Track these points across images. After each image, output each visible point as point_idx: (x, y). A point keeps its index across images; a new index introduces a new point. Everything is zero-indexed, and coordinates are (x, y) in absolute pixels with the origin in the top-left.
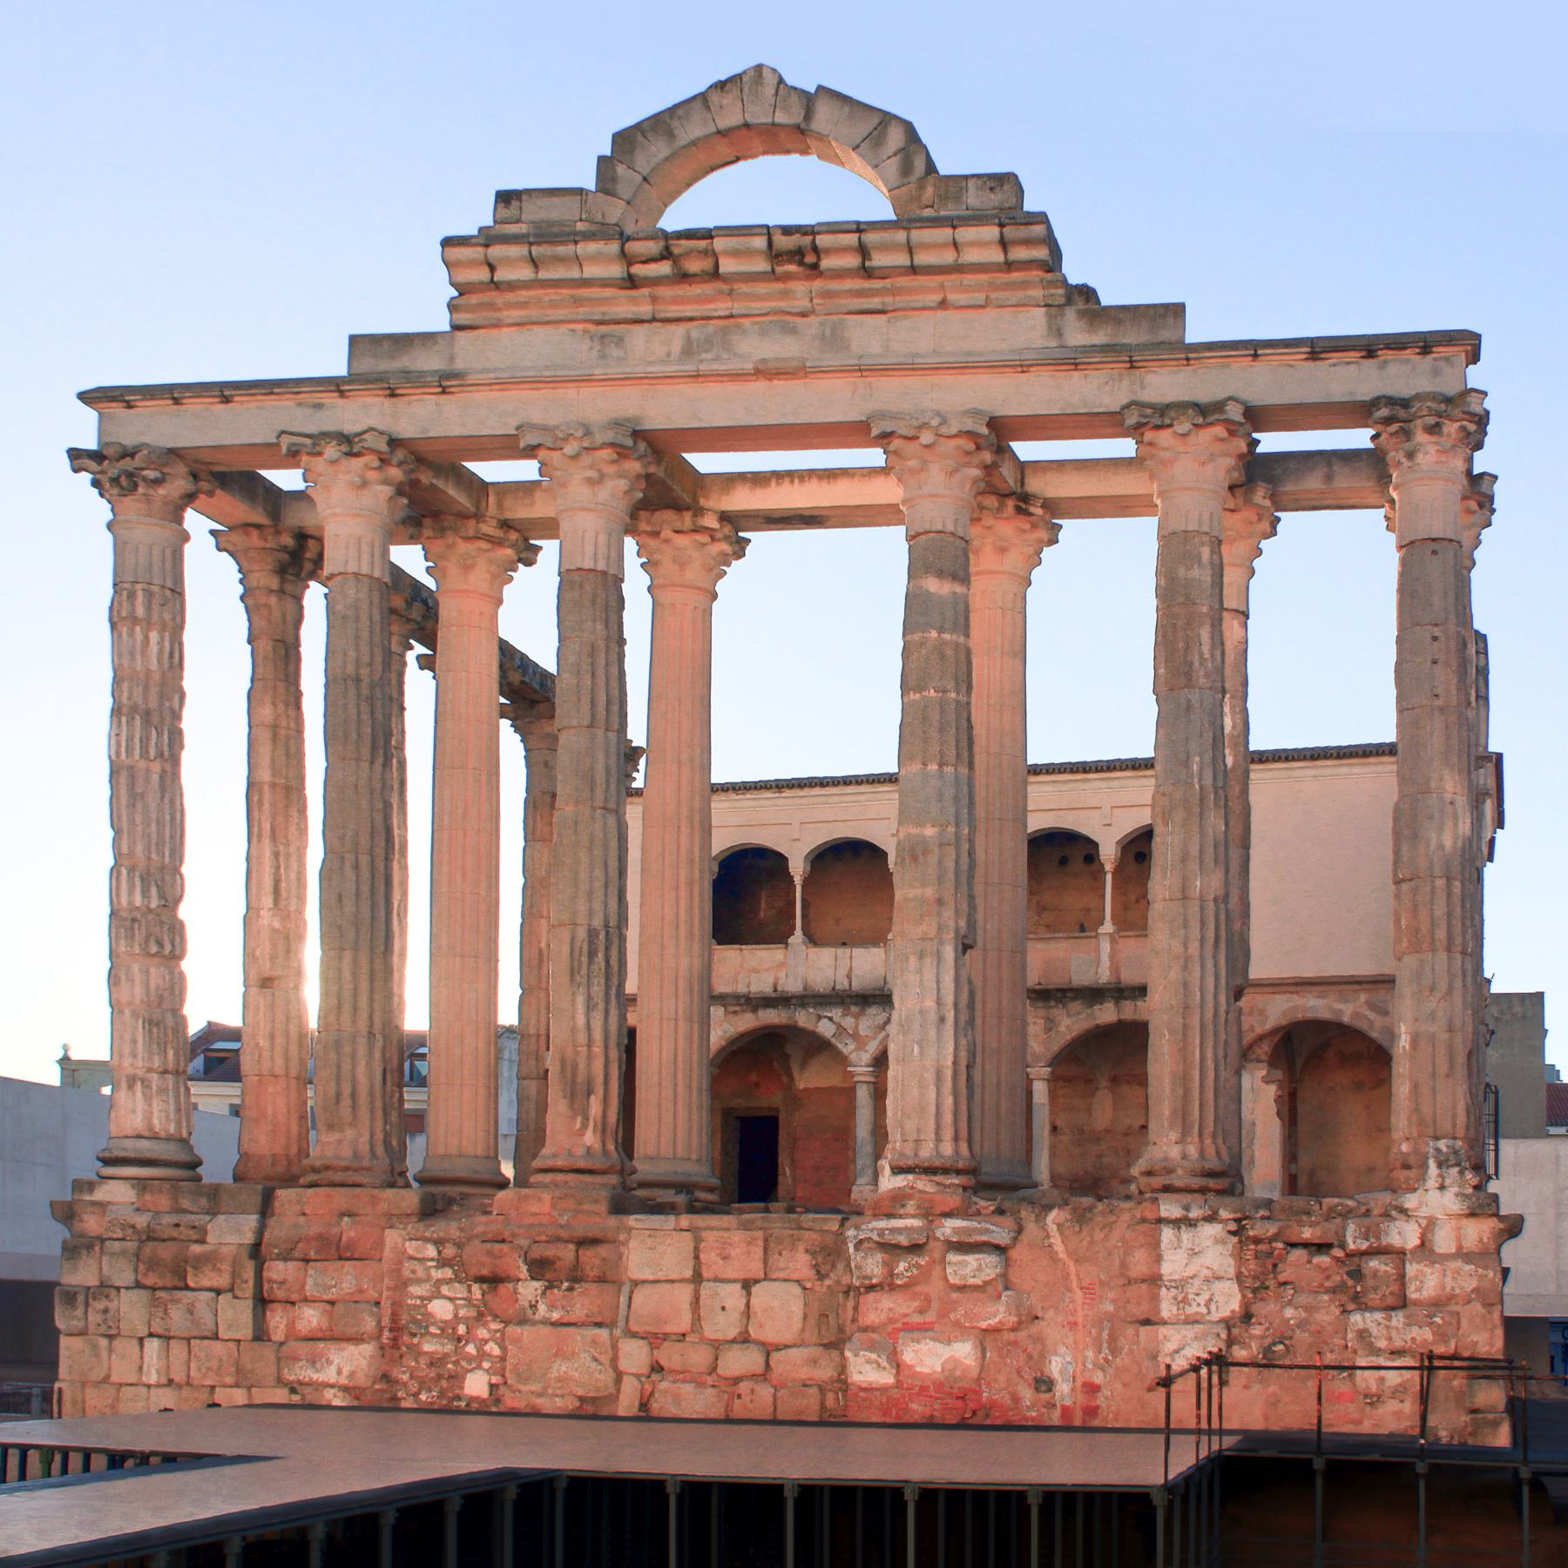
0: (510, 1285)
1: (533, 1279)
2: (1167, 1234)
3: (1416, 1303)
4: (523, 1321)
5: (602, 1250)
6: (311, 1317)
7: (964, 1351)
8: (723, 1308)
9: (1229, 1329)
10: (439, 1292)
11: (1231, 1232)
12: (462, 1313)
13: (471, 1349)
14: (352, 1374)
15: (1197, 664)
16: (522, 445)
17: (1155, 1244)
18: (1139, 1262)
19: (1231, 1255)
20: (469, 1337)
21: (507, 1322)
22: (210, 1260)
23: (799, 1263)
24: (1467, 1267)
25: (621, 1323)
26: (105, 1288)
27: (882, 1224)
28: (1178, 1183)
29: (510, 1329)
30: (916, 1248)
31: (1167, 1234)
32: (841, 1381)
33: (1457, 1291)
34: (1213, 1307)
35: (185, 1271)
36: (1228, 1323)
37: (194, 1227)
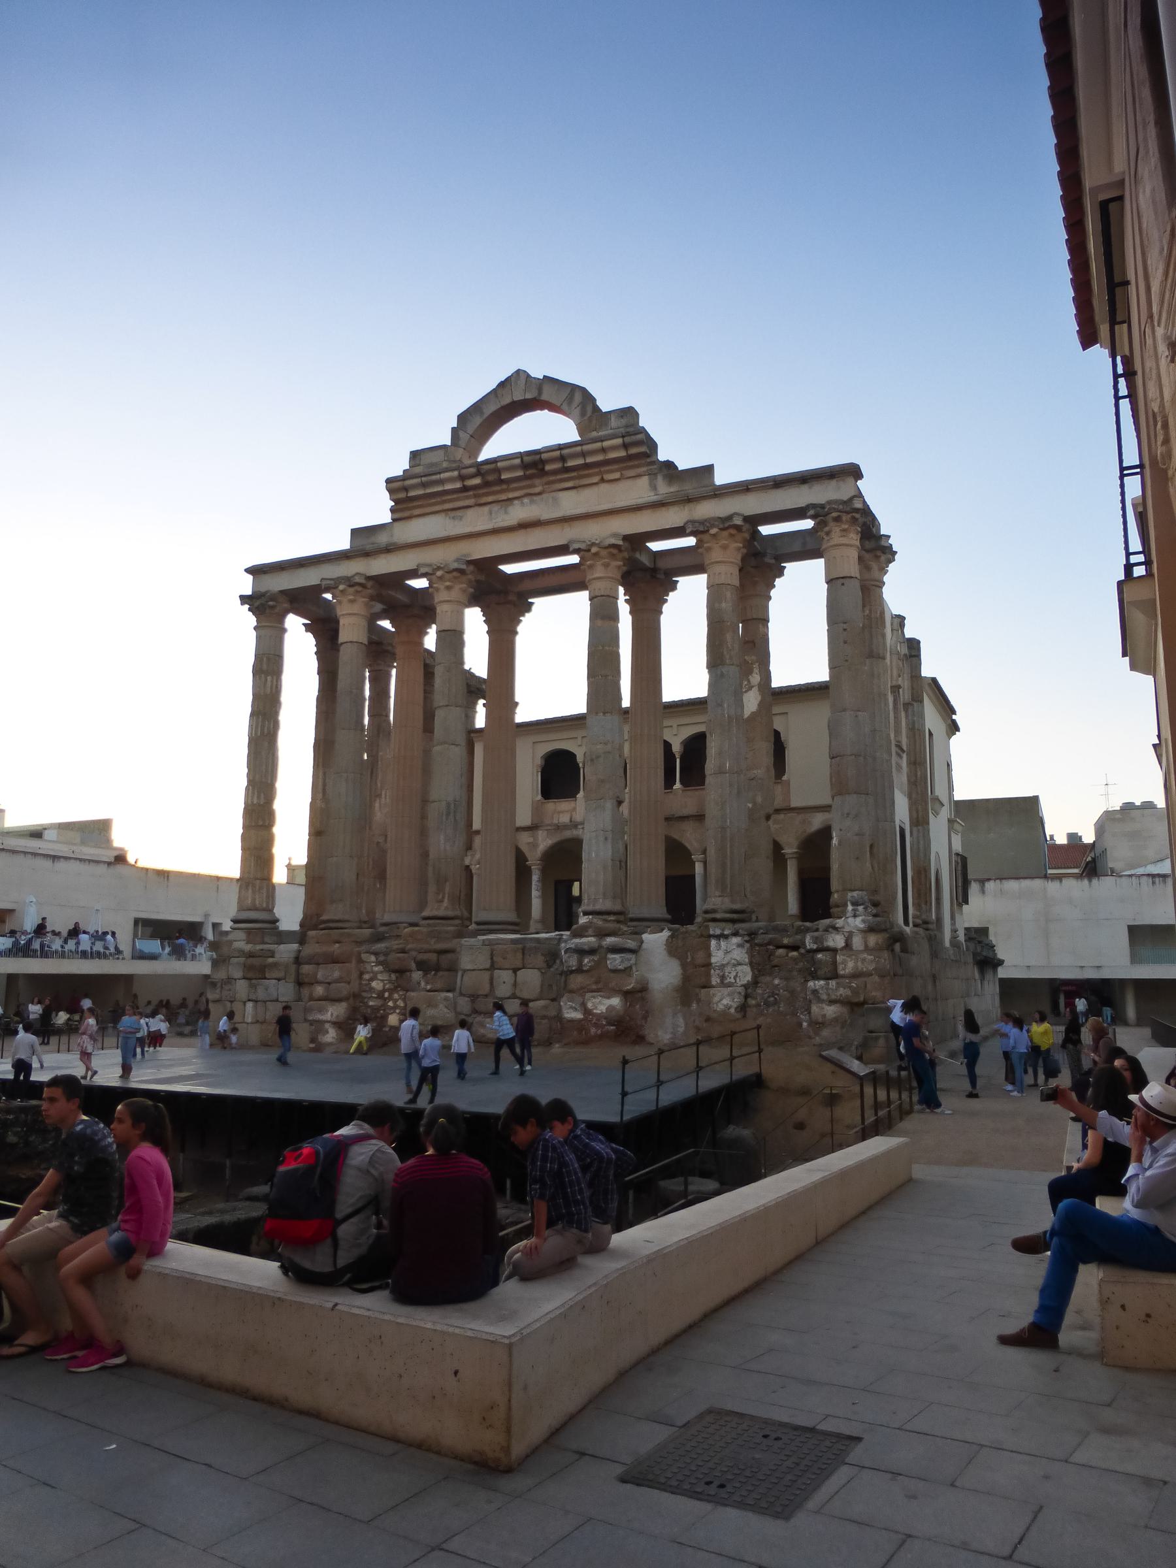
0: (408, 973)
1: (418, 970)
2: (713, 942)
3: (843, 977)
4: (413, 991)
5: (449, 956)
6: (319, 990)
7: (616, 1001)
8: (504, 983)
9: (746, 989)
10: (377, 977)
11: (747, 941)
12: (387, 986)
13: (391, 1004)
14: (337, 1016)
15: (725, 653)
16: (420, 573)
17: (708, 948)
18: (700, 957)
19: (747, 953)
20: (390, 998)
21: (407, 991)
23: (540, 960)
24: (870, 957)
25: (458, 990)
26: (230, 980)
27: (577, 940)
28: (718, 916)
29: (408, 994)
30: (592, 951)
31: (713, 942)
32: (559, 1017)
33: (865, 969)
34: (738, 980)
36: (746, 986)
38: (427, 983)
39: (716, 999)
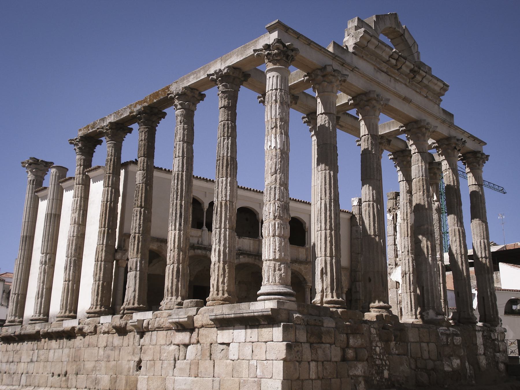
0: (389, 343)
1: (394, 341)
8: (425, 350)
22: (328, 332)
35: (322, 337)
37: (320, 321)
38: (396, 349)
39: (481, 361)
